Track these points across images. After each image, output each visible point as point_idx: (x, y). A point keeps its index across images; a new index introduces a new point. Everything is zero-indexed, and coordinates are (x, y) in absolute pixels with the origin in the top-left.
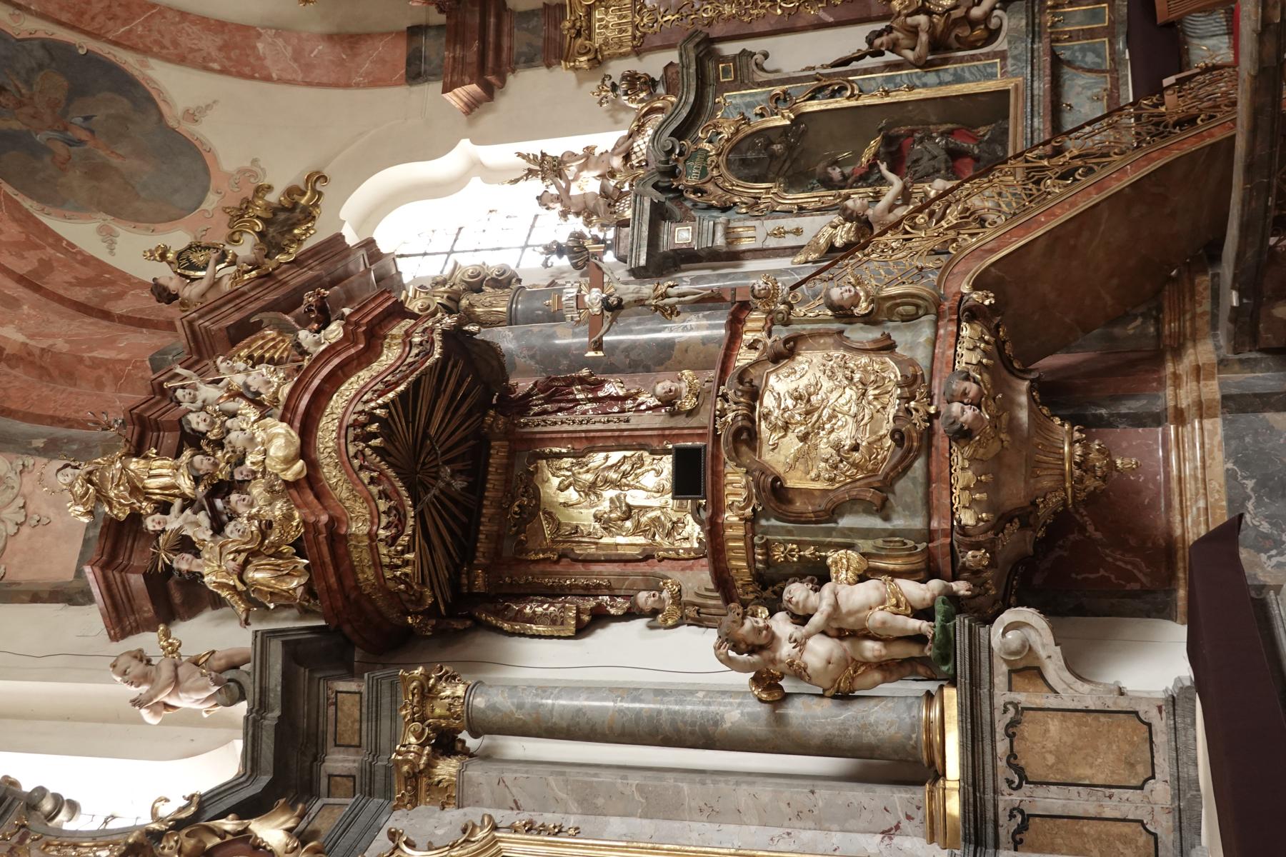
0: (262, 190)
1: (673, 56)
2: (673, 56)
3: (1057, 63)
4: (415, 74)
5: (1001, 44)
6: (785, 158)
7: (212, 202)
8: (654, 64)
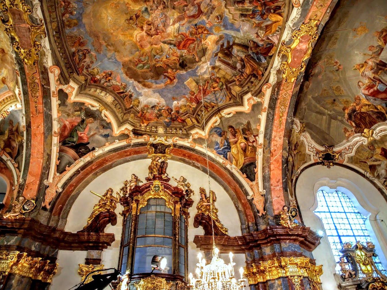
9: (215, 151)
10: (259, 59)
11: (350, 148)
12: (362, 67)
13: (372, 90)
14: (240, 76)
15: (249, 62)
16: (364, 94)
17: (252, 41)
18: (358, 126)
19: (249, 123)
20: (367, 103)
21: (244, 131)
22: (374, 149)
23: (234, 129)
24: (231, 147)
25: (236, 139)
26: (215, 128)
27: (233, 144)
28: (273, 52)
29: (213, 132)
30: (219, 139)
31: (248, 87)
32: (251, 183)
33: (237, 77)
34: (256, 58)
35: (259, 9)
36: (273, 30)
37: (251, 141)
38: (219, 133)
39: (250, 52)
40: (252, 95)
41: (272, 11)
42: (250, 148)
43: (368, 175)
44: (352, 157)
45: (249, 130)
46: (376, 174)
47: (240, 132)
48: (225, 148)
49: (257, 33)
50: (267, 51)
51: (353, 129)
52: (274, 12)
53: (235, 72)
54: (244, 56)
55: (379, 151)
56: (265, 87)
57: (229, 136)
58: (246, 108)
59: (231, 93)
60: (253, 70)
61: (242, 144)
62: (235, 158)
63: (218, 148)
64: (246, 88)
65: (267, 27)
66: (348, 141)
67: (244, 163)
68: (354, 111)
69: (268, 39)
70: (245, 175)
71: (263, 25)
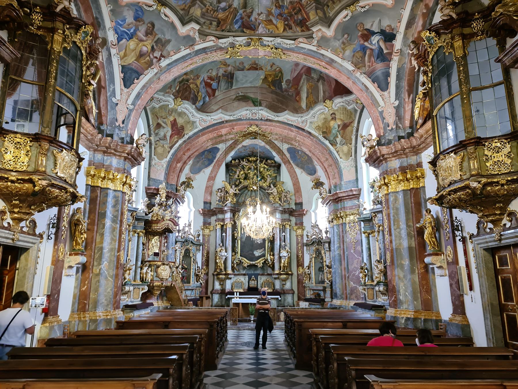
0: (192, 181)
1: (201, 241)
2: (201, 241)
3: (192, 290)
4: (205, 203)
5: (196, 283)
6: (187, 255)
7: (192, 175)
8: (201, 238)
9: (114, 24)
10: (236, 23)
11: (159, 101)
12: (224, 65)
13: (209, 81)
14: (212, 9)
15: (231, 13)
16: (204, 78)
17: (253, 11)
18: (178, 92)
19: (169, 41)
20: (198, 84)
21: (158, 41)
22: (170, 115)
23: (153, 29)
24: (132, 38)
25: (144, 38)
26: (141, 7)
27: (137, 39)
28: (248, 32)
29: (134, 8)
30: (130, 19)
31: (204, 23)
32: (124, 88)
33: (211, 7)
34: (237, 18)
35: (286, 11)
36: (268, 27)
37: (155, 55)
38: (137, 16)
39: (241, 11)
40: (199, 30)
41: (286, 23)
42: (148, 58)
43: (152, 128)
44: (155, 107)
45: (162, 46)
46: (156, 131)
47: (154, 38)
48: (126, 33)
49: (262, 13)
50: (248, 27)
51: (174, 91)
52: (285, 25)
53: (215, 4)
54: (235, 6)
55: (172, 119)
56: (213, 38)
57: (143, 29)
58: (183, 30)
59: (190, 7)
60: (225, 20)
61: (145, 49)
62: (126, 50)
63: (121, 25)
64: (202, 20)
65: (271, 21)
66: (164, 95)
67: (130, 64)
68: (188, 80)
69: (259, 24)
70: (122, 75)
71: (271, 17)
